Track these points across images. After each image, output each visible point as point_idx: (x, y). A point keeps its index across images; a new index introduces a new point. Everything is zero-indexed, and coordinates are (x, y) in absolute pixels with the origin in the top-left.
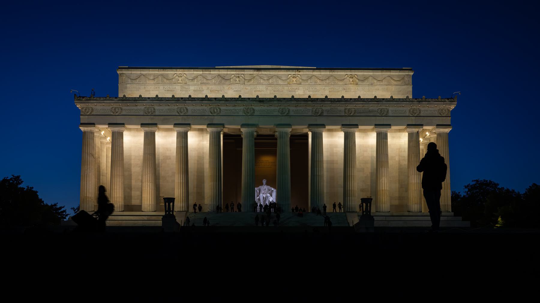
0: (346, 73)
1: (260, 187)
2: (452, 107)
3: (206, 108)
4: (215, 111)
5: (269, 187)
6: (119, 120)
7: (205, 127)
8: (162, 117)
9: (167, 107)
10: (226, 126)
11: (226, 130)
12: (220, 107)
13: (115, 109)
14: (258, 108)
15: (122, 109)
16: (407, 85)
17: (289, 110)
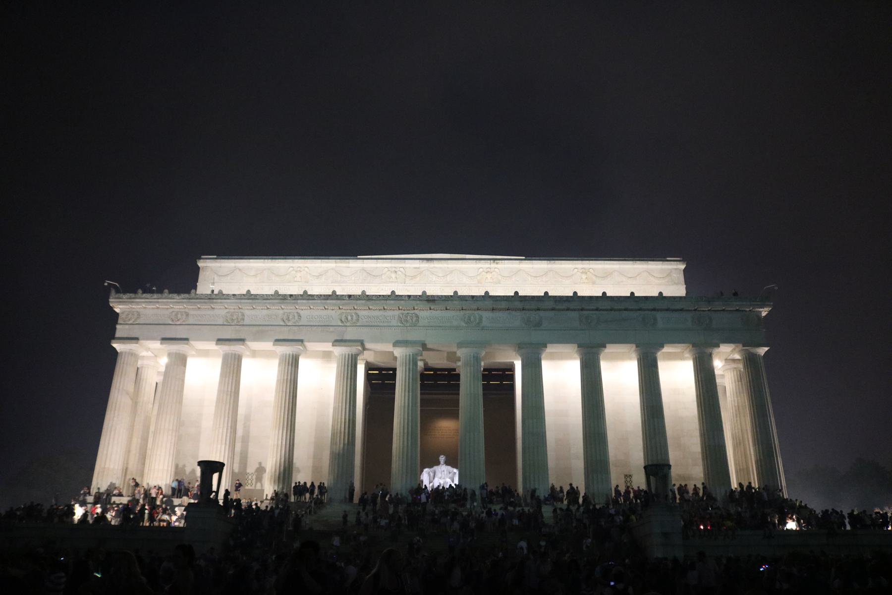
0: (574, 266)
1: (435, 468)
2: (764, 314)
3: (333, 313)
4: (349, 318)
5: (449, 467)
6: (180, 332)
7: (328, 347)
8: (255, 329)
9: (265, 312)
10: (368, 345)
11: (369, 356)
12: (358, 312)
13: (176, 315)
14: (425, 314)
15: (187, 315)
16: (677, 284)
17: (481, 318)
